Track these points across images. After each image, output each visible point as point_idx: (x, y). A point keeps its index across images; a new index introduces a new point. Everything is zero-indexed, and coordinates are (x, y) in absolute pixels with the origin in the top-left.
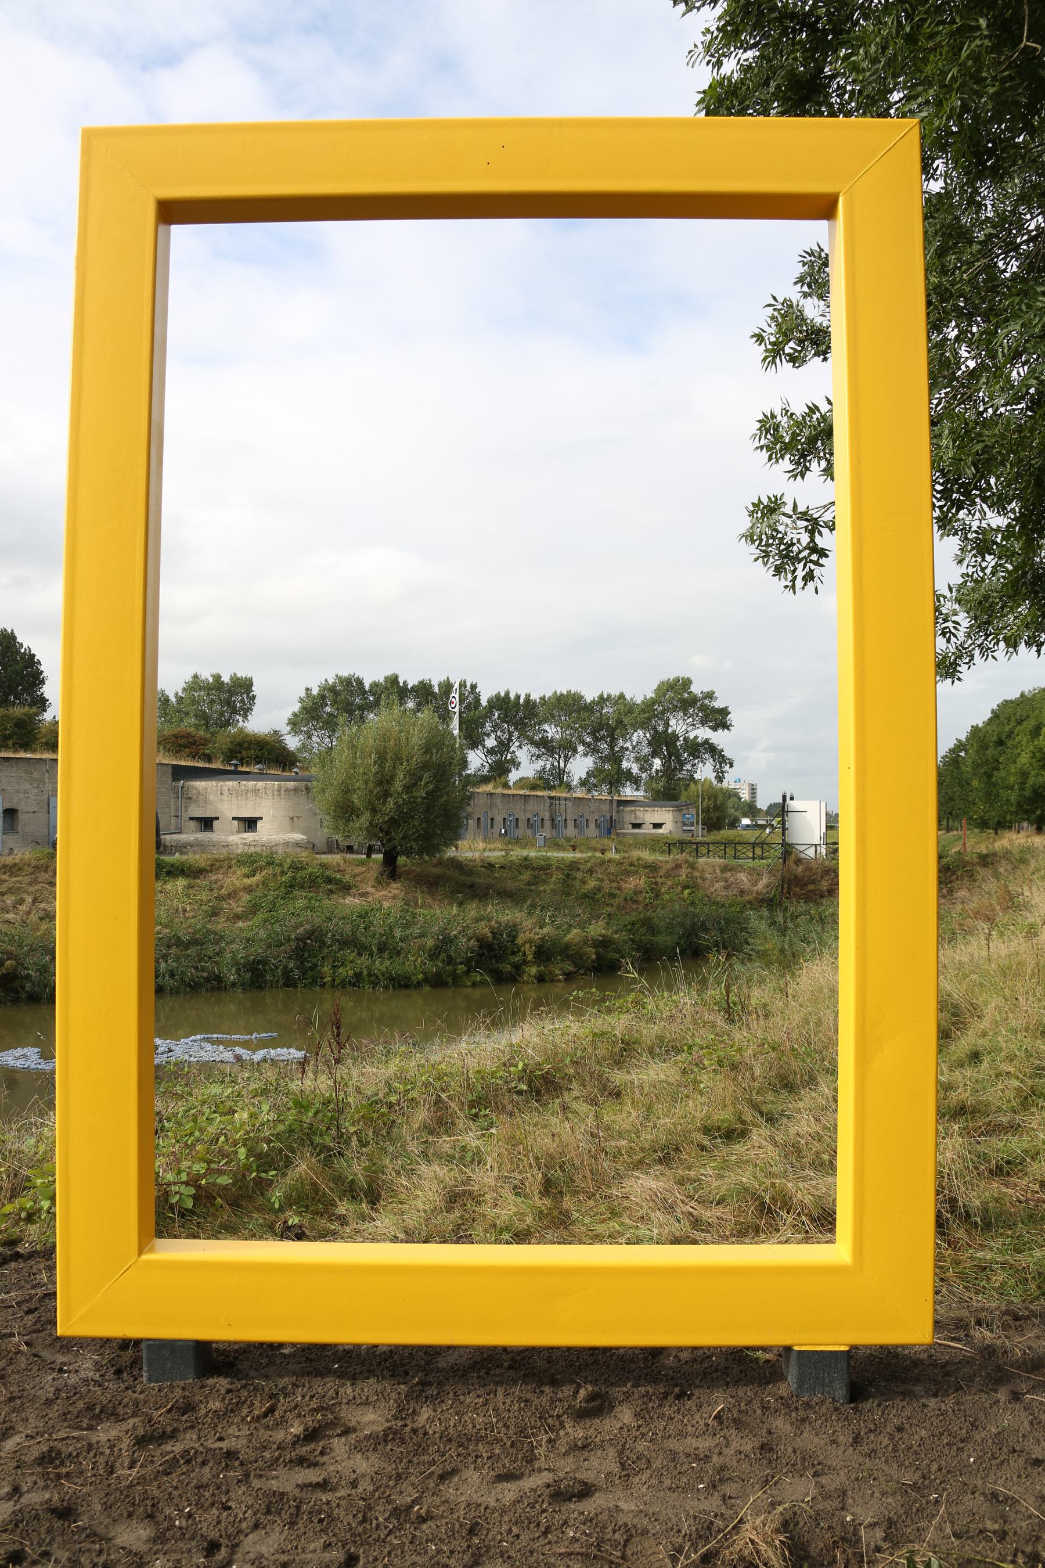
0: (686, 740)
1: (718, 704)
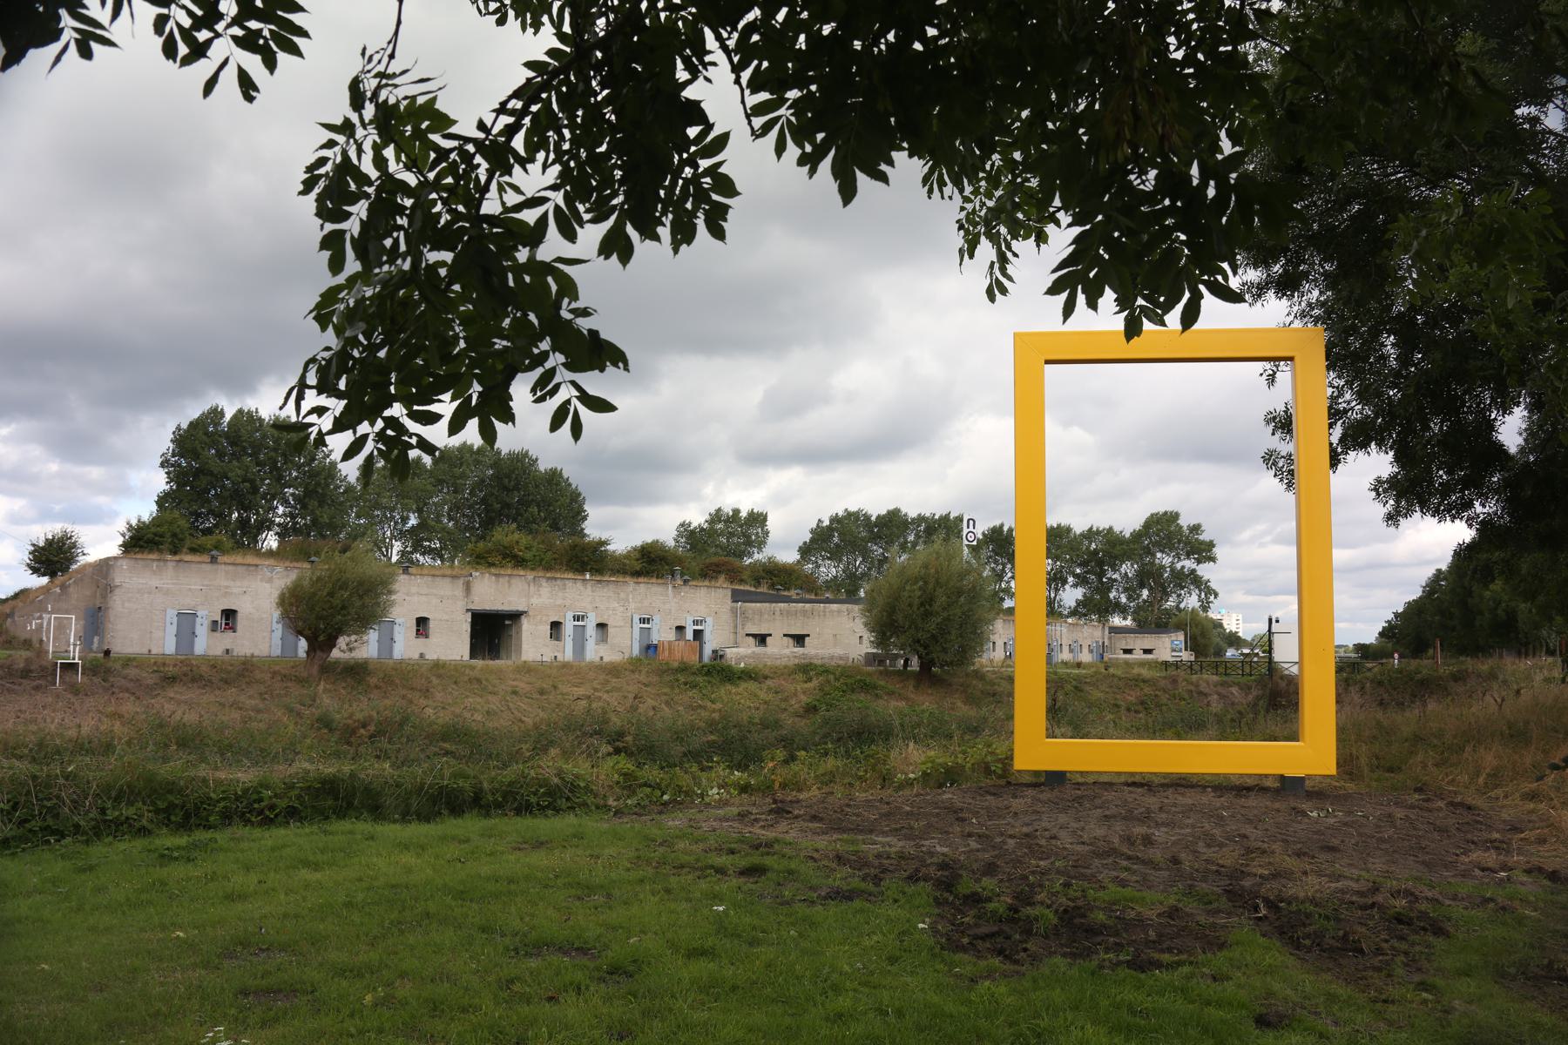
0: (1173, 570)
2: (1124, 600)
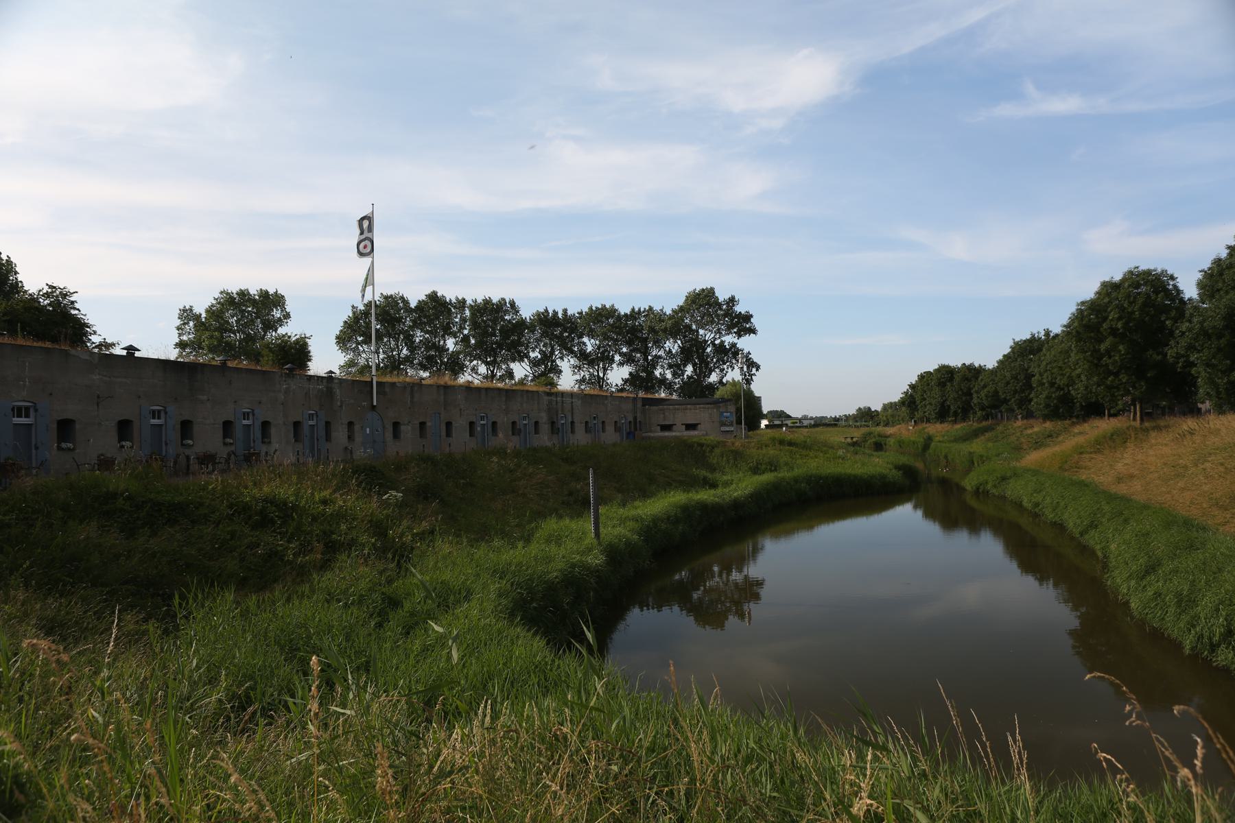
1: (739, 309)
2: (669, 376)
